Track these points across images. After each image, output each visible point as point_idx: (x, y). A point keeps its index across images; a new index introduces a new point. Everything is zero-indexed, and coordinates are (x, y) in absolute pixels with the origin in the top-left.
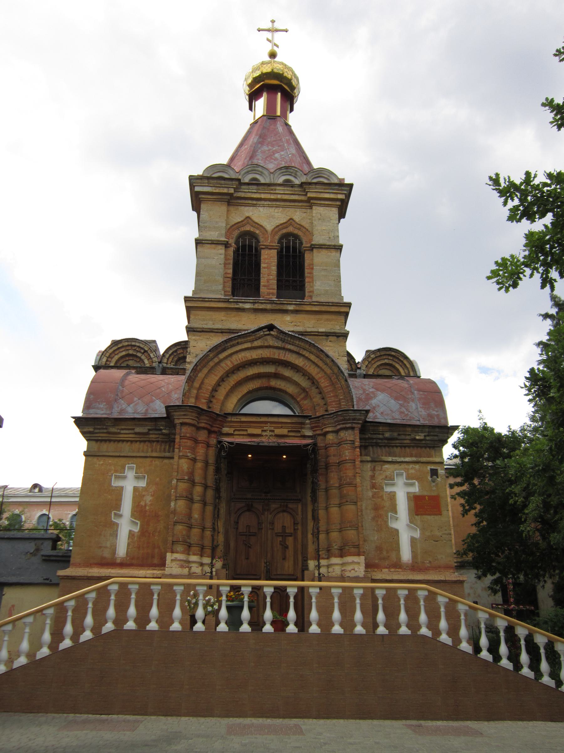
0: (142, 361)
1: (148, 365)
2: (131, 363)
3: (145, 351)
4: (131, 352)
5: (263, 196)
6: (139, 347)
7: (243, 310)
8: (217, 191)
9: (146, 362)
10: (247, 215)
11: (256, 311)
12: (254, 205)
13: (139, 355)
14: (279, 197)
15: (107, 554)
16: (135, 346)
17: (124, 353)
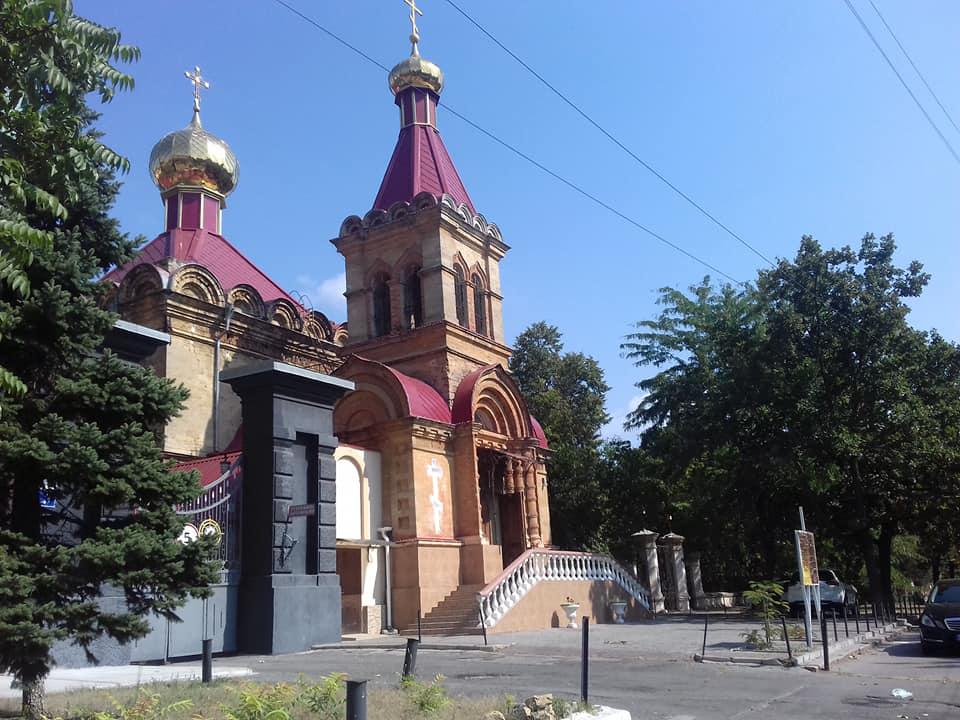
0: (205, 296)
1: (211, 302)
2: (190, 293)
3: (210, 284)
4: (195, 281)
5: (469, 236)
6: (204, 277)
7: (468, 340)
8: (451, 222)
9: (210, 297)
10: (459, 248)
11: (475, 343)
12: (461, 241)
13: (202, 286)
14: (475, 240)
15: (431, 528)
16: (200, 275)
17: (188, 280)
